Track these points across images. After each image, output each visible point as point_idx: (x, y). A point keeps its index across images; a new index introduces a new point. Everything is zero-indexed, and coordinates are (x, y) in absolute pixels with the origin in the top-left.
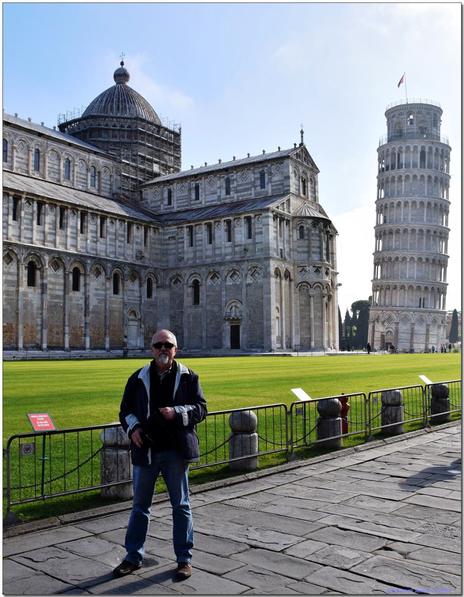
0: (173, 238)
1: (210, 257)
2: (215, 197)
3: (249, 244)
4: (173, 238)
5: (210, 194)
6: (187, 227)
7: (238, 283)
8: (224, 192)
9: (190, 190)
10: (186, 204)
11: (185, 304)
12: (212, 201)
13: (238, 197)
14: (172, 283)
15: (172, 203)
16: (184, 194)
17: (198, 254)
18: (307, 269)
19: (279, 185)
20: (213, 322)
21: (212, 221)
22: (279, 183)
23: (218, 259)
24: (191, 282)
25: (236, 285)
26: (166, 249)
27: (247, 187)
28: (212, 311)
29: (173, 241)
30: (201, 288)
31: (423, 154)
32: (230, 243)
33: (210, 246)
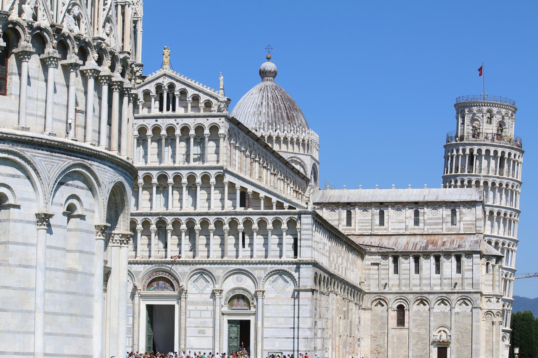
0: (377, 264)
1: (417, 286)
2: (403, 226)
3: (458, 279)
4: (377, 264)
5: (396, 222)
6: (392, 256)
7: (446, 311)
8: (412, 222)
9: (372, 215)
10: (368, 228)
11: (390, 326)
12: (399, 229)
13: (428, 229)
14: (373, 306)
15: (353, 224)
16: (366, 218)
17: (403, 282)
18: (492, 299)
19: (470, 224)
20: (420, 343)
21: (421, 254)
22: (470, 222)
23: (426, 289)
24: (395, 306)
25: (444, 312)
26: (368, 274)
27: (437, 221)
28: (419, 334)
29: (376, 267)
30: (406, 313)
31: (502, 158)
32: (439, 276)
33: (418, 275)
